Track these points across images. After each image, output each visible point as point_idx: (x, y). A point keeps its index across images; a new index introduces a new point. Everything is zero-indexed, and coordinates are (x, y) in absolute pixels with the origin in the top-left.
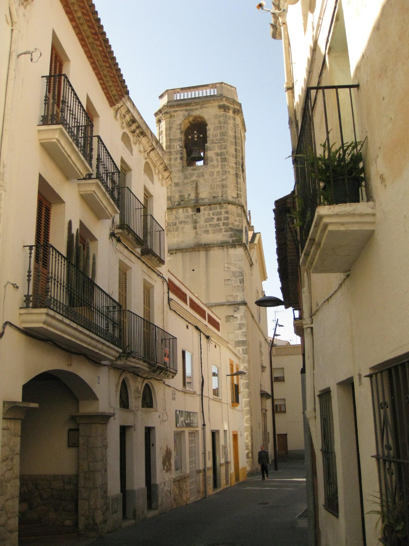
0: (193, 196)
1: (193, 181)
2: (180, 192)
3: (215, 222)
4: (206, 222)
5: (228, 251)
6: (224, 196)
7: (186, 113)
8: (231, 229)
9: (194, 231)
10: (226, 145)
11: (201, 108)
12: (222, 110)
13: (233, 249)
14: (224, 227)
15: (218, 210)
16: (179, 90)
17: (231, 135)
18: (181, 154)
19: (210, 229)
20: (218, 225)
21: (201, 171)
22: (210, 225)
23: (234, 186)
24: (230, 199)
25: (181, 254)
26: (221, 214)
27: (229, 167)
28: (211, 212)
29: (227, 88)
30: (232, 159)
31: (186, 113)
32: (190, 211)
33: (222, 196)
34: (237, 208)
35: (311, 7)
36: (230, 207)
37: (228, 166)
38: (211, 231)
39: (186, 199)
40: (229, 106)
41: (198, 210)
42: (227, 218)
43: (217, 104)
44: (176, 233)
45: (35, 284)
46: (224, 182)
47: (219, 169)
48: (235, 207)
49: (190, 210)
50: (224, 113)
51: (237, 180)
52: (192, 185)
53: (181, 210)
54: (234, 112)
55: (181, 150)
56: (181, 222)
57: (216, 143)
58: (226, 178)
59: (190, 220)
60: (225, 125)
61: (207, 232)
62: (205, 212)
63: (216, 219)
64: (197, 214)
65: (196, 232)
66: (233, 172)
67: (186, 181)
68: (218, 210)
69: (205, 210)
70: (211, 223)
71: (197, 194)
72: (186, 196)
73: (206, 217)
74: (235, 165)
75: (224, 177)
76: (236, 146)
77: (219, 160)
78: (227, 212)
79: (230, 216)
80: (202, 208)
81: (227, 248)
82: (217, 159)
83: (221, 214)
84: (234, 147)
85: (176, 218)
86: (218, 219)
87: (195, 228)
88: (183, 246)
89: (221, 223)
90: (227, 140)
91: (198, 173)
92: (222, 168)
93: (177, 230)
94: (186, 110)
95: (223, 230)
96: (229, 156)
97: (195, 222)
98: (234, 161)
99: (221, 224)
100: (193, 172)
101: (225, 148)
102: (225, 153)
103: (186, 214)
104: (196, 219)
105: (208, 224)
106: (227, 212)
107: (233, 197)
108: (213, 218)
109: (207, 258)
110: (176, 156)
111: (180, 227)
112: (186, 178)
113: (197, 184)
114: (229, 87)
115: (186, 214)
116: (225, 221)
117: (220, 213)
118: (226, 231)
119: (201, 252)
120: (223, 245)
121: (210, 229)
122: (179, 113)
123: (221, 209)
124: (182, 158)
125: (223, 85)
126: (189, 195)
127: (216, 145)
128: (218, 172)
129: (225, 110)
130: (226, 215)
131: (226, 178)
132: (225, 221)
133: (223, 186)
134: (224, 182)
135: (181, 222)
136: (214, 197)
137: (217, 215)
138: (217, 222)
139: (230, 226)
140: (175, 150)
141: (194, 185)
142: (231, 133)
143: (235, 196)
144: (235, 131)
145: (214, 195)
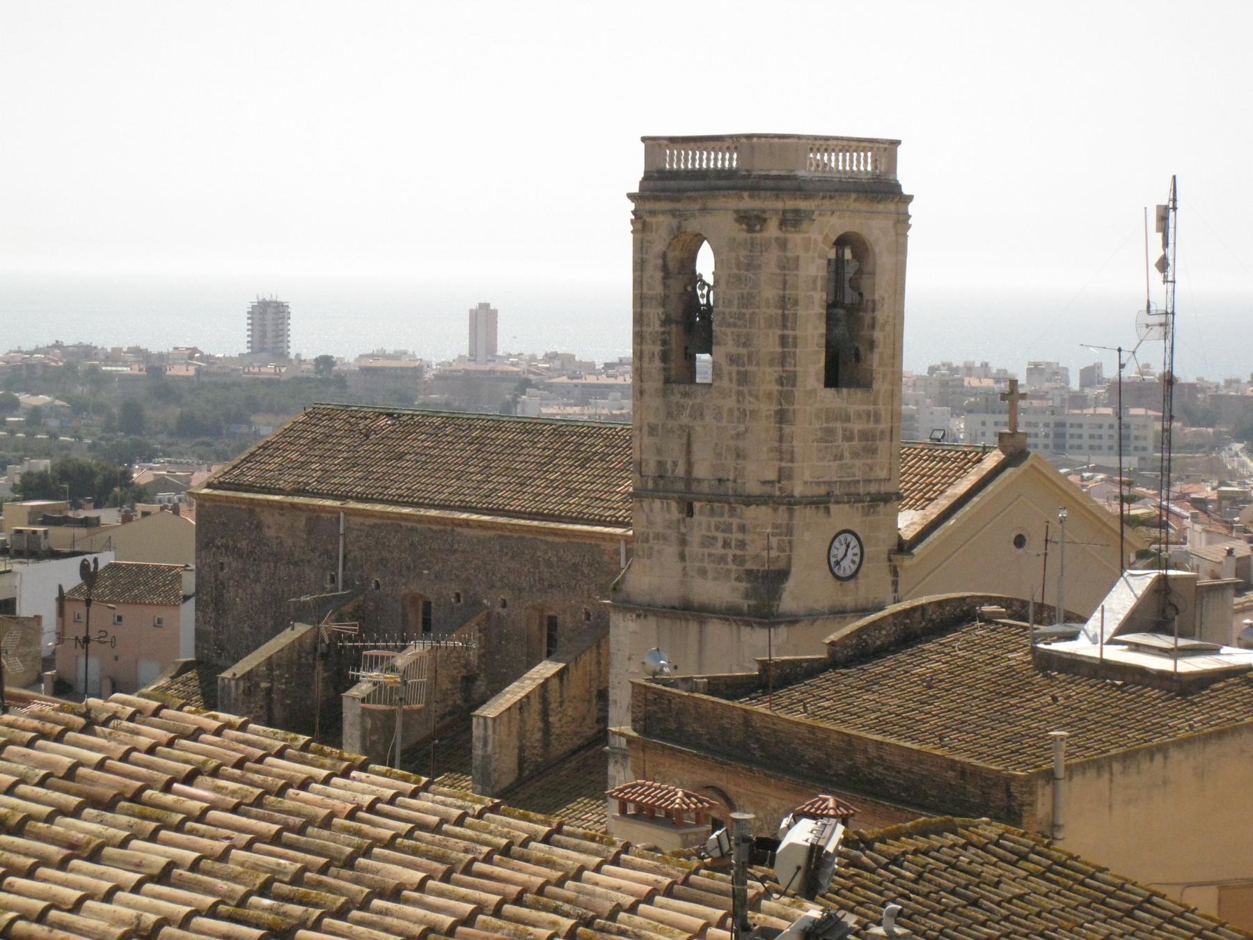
0: (681, 471)
1: (682, 427)
2: (659, 452)
3: (718, 550)
4: (703, 545)
5: (739, 632)
6: (739, 481)
7: (674, 222)
8: (749, 573)
9: (680, 566)
10: (748, 334)
11: (704, 210)
12: (744, 226)
13: (748, 629)
14: (734, 567)
15: (726, 518)
16: (666, 142)
17: (767, 299)
18: (664, 343)
19: (709, 566)
20: (723, 559)
21: (698, 400)
22: (710, 555)
23: (771, 450)
24: (753, 488)
25: (654, 619)
26: (731, 532)
27: (757, 397)
28: (714, 520)
29: (771, 145)
30: (768, 370)
31: (674, 222)
32: (675, 513)
33: (735, 481)
34: (775, 510)
35: (13, 870)
36: (752, 512)
37: (751, 395)
38: (710, 575)
39: (669, 474)
40: (764, 211)
41: (690, 513)
42: (742, 545)
43: (734, 204)
44: (648, 562)
45: (371, 666)
46: (741, 444)
47: (731, 402)
48: (769, 511)
49: (674, 505)
50: (748, 236)
51: (781, 429)
52: (680, 437)
53: (657, 504)
54: (783, 223)
55: (663, 333)
56: (657, 537)
57: (729, 325)
58: (746, 431)
59: (673, 535)
60: (750, 275)
61: (703, 572)
62: (702, 521)
63: (720, 544)
64: (688, 519)
65: (684, 568)
66: (768, 408)
67: (671, 423)
68: (726, 518)
69: (701, 513)
70: (713, 551)
71: (689, 464)
72: (669, 466)
73: (704, 532)
74: (776, 388)
75: (741, 428)
76: (784, 327)
77: (734, 375)
78: (742, 529)
79: (748, 538)
80: (697, 505)
81: (738, 626)
82: (730, 374)
83: (731, 532)
84: (779, 332)
85: (650, 523)
86: (726, 544)
87: (682, 557)
88: (660, 598)
89: (730, 553)
90: (752, 321)
91: (692, 406)
92: (738, 401)
93: (650, 556)
94: (673, 213)
95: (733, 576)
96: (758, 364)
97: (683, 542)
98: (776, 376)
99: (730, 559)
100: (682, 401)
101: (745, 345)
102: (746, 359)
103: (668, 516)
104: (684, 534)
105: (706, 551)
106: (742, 529)
107: (764, 483)
108: (715, 539)
109: (700, 642)
110: (651, 347)
111: (656, 548)
112: (669, 415)
113: (689, 436)
114: (776, 140)
115: (668, 516)
116: (739, 552)
117: (728, 529)
118: (738, 579)
119: (691, 623)
120: (730, 614)
121: (709, 566)
122: (661, 218)
123: (731, 516)
124: (665, 357)
125: (755, 140)
126: (675, 464)
127: (729, 330)
128: (731, 411)
129: (751, 230)
130: (740, 536)
131: (746, 431)
132: (739, 552)
133: (740, 455)
134: (741, 444)
135: (657, 537)
136: (720, 480)
137: (723, 531)
138: (724, 552)
139: (749, 565)
140: (651, 329)
141: (684, 441)
142: (769, 293)
143: (772, 476)
144: (785, 283)
145: (721, 475)
